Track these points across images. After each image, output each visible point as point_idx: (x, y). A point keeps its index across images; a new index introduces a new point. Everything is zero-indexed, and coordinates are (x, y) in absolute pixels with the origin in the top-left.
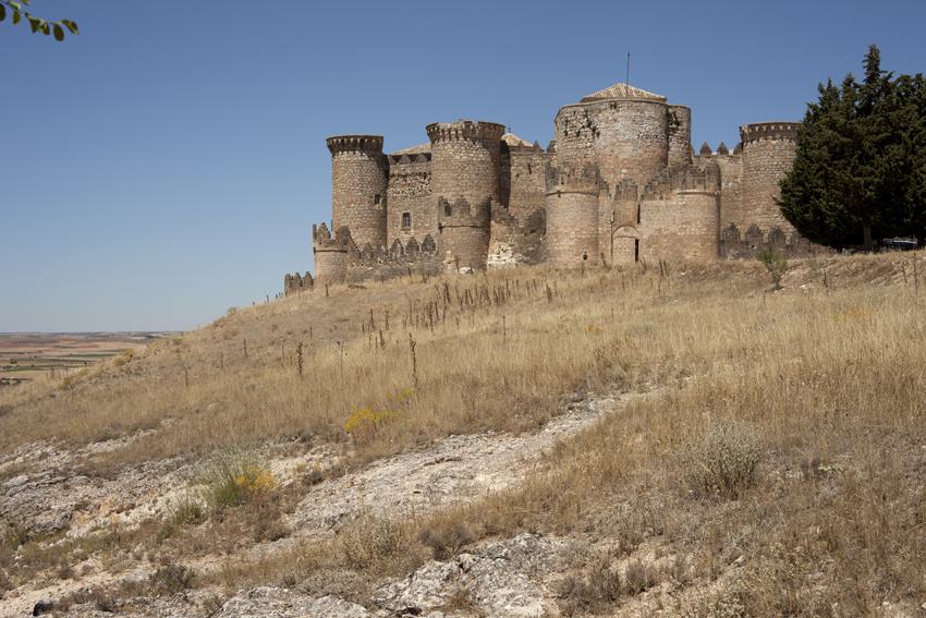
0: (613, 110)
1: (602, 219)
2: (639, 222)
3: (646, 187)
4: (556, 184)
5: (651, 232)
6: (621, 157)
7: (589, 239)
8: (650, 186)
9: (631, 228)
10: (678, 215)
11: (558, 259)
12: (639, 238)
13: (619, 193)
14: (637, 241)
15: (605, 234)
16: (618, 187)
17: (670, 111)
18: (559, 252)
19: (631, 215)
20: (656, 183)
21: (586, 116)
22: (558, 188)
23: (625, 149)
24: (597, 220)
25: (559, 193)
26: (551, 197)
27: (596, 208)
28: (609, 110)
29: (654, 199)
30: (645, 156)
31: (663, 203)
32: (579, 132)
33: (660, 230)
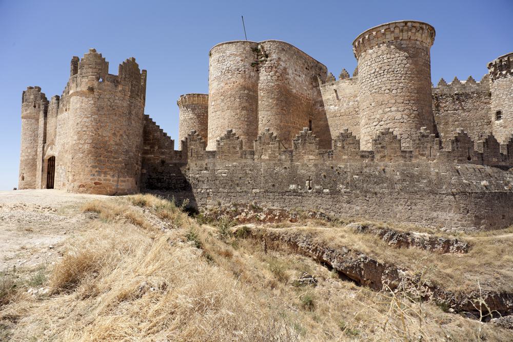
30: (227, 87)
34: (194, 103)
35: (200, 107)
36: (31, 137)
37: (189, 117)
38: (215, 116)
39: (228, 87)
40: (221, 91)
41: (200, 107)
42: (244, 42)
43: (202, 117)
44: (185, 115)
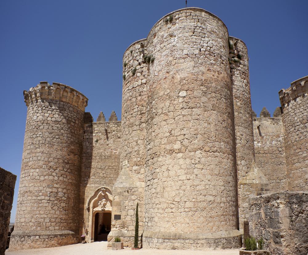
0: (169, 25)
6: (178, 77)
21: (143, 51)
23: (184, 66)
28: (165, 28)
30: (209, 75)
32: (135, 70)
34: (64, 100)
35: (71, 109)
37: (54, 119)
38: (191, 115)
39: (212, 76)
40: (200, 77)
41: (71, 109)
42: (224, 24)
43: (73, 124)
44: (47, 115)
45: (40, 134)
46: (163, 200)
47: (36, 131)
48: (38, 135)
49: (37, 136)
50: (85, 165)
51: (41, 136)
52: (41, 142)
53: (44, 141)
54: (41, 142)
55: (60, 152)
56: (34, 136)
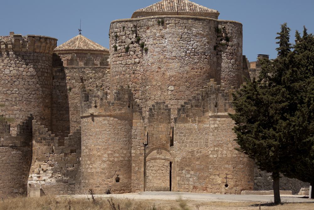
1: (135, 142)
2: (172, 145)
3: (179, 110)
4: (89, 107)
5: (184, 154)
7: (122, 161)
8: (182, 109)
9: (164, 151)
10: (211, 138)
11: (91, 181)
12: (172, 159)
13: (151, 115)
14: (171, 163)
15: (137, 156)
16: (151, 109)
17: (220, 26)
18: (92, 174)
19: (163, 137)
20: (189, 106)
22: (91, 111)
24: (130, 142)
25: (92, 116)
26: (85, 120)
27: (129, 131)
29: (187, 122)
31: (195, 126)
33: (192, 152)
36: (126, 138)
45: (16, 91)
46: (156, 164)
47: (11, 87)
48: (13, 92)
49: (12, 92)
50: (57, 117)
51: (17, 92)
52: (18, 99)
53: (21, 98)
54: (18, 99)
55: (37, 109)
56: (9, 92)
